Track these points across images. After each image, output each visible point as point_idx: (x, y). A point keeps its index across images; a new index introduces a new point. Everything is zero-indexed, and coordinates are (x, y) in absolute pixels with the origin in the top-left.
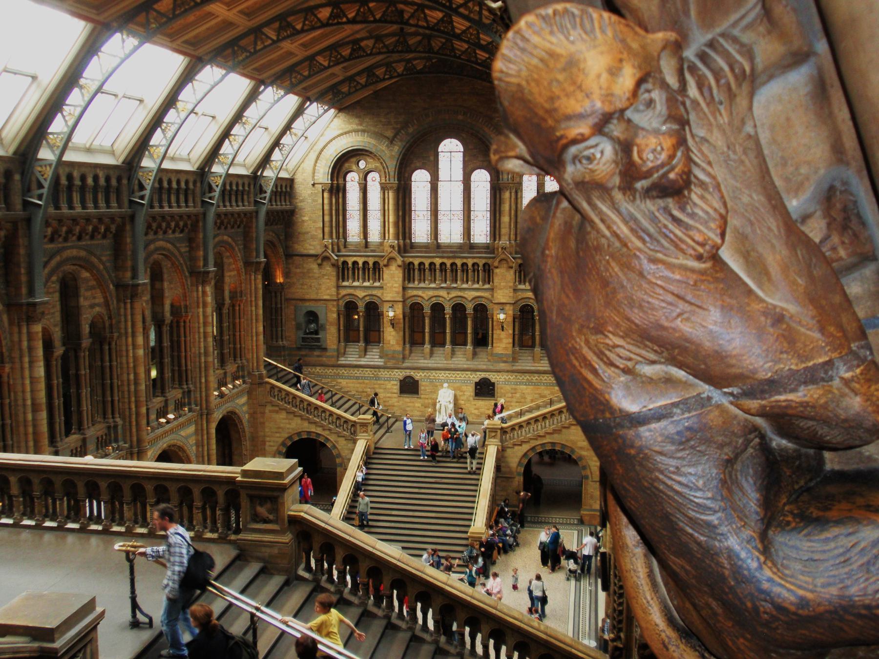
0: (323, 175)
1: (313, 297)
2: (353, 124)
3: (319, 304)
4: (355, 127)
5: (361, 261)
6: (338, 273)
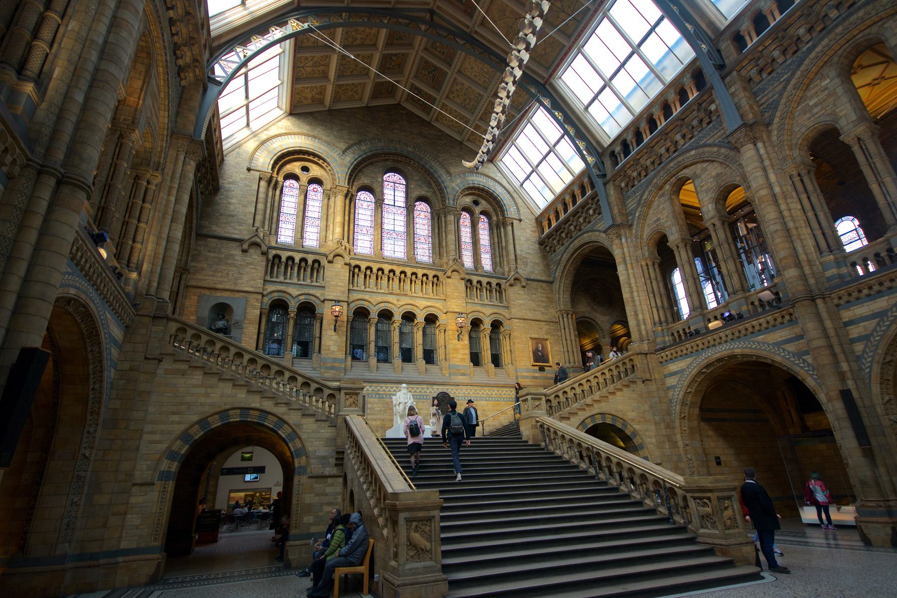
0: (264, 161)
1: (227, 287)
2: (305, 128)
3: (237, 295)
4: (305, 131)
5: (297, 257)
6: (267, 266)
